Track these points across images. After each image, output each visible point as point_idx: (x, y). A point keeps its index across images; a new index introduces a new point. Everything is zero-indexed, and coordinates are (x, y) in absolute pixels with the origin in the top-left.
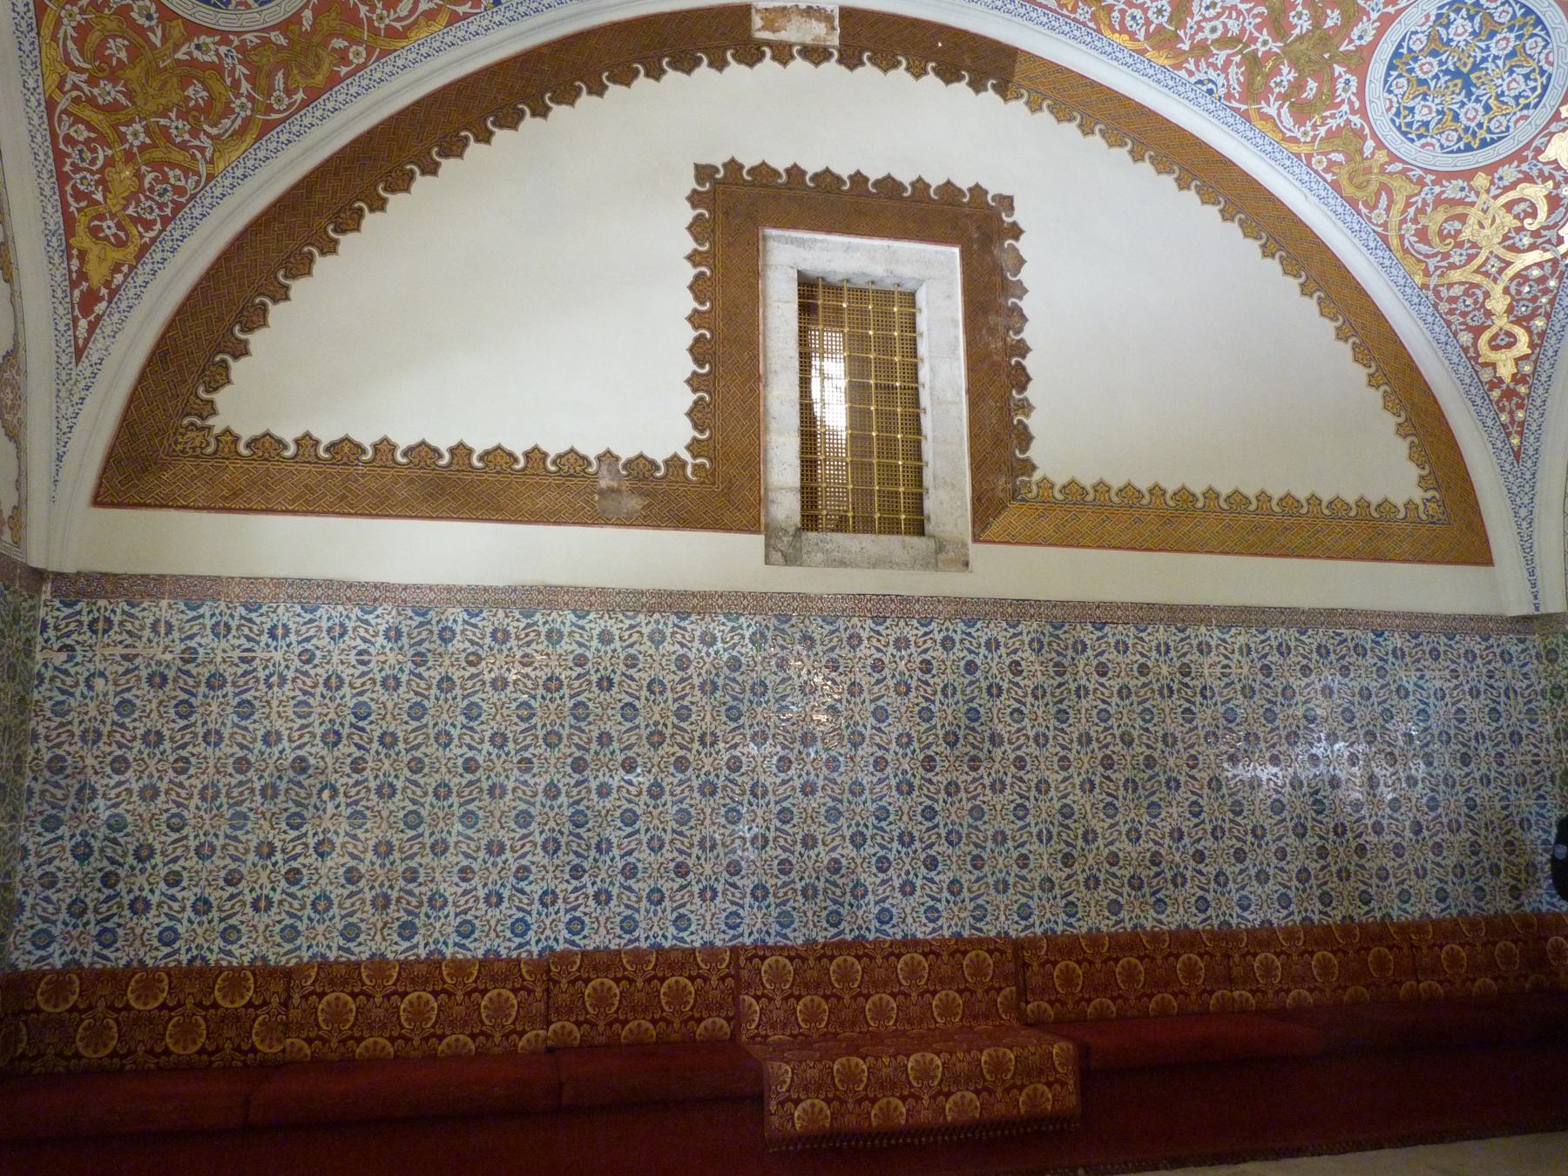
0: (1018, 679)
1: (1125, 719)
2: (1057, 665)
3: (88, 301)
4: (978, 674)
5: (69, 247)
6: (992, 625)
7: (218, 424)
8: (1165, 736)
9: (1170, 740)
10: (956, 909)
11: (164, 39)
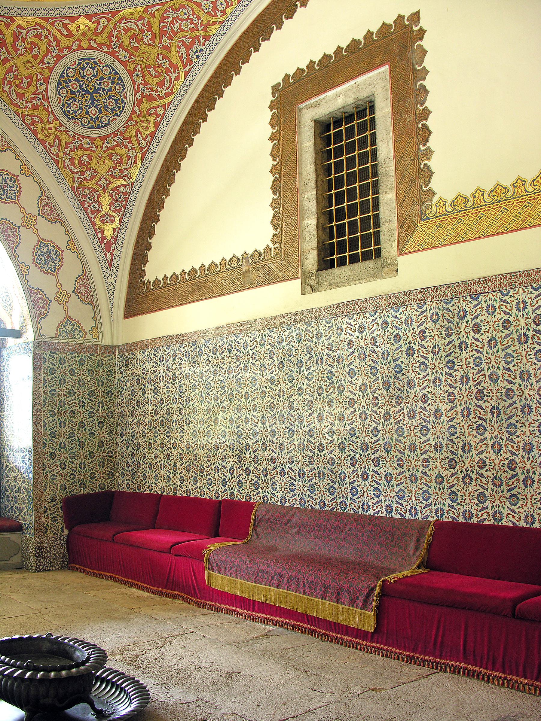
0: (423, 342)
1: (493, 363)
2: (447, 329)
3: (108, 246)
4: (401, 342)
5: (96, 230)
6: (409, 309)
7: (146, 278)
8: (522, 373)
9: (525, 376)
10: (389, 491)
11: (97, 148)
